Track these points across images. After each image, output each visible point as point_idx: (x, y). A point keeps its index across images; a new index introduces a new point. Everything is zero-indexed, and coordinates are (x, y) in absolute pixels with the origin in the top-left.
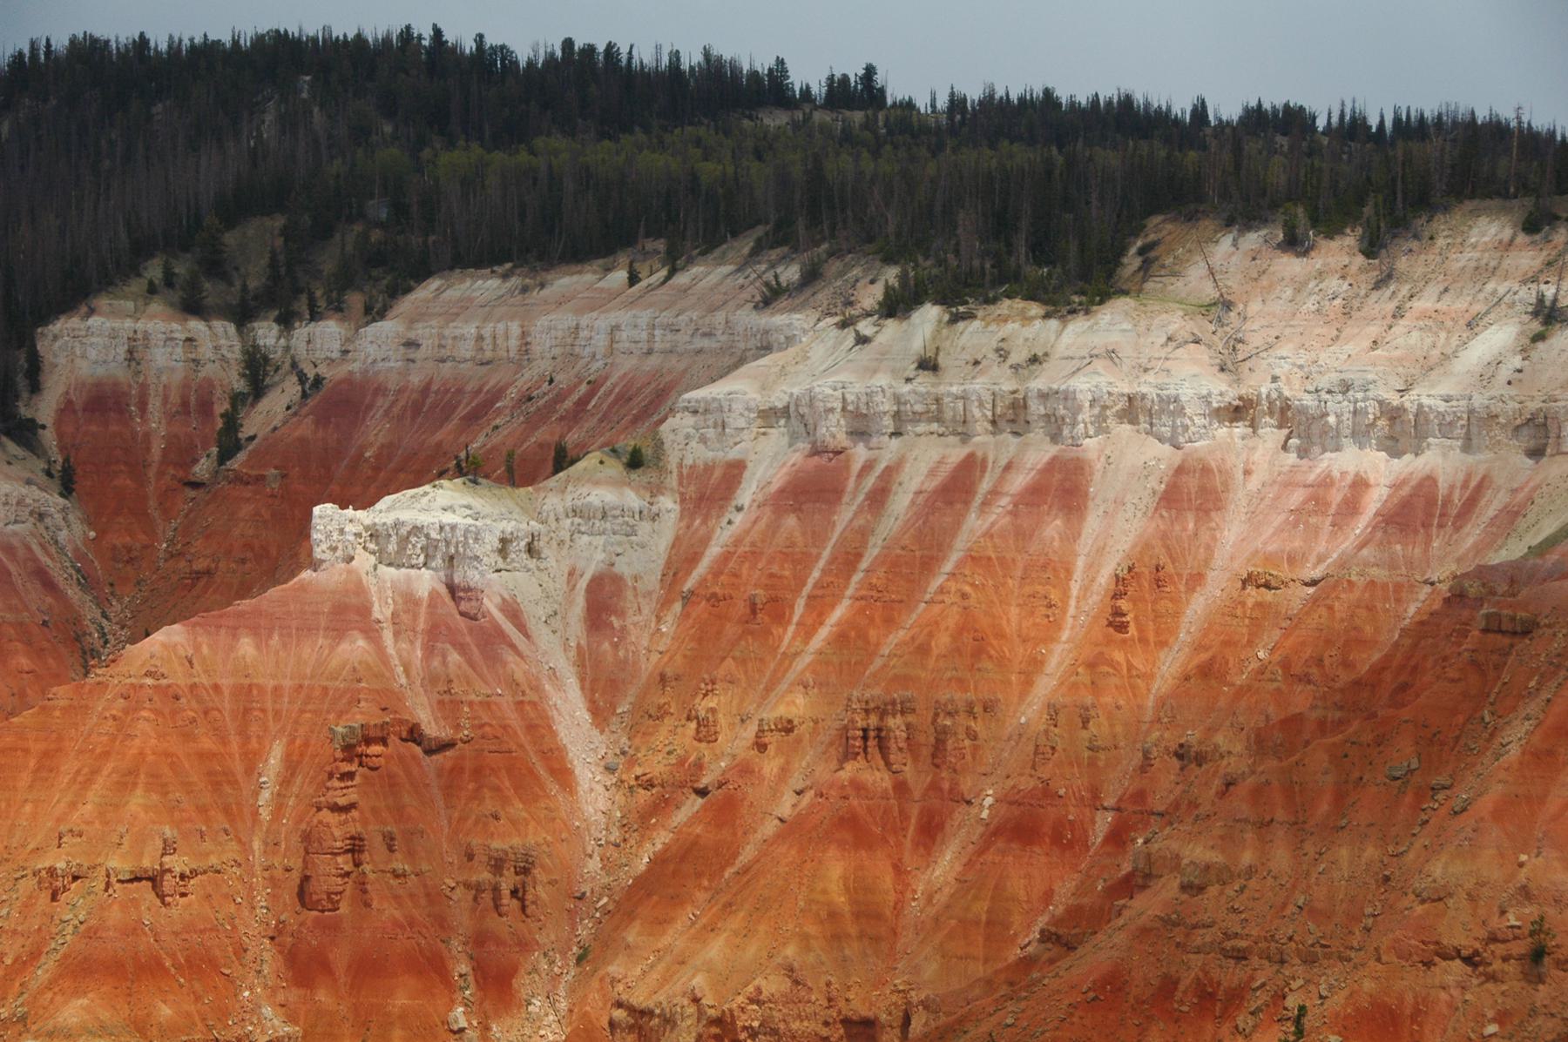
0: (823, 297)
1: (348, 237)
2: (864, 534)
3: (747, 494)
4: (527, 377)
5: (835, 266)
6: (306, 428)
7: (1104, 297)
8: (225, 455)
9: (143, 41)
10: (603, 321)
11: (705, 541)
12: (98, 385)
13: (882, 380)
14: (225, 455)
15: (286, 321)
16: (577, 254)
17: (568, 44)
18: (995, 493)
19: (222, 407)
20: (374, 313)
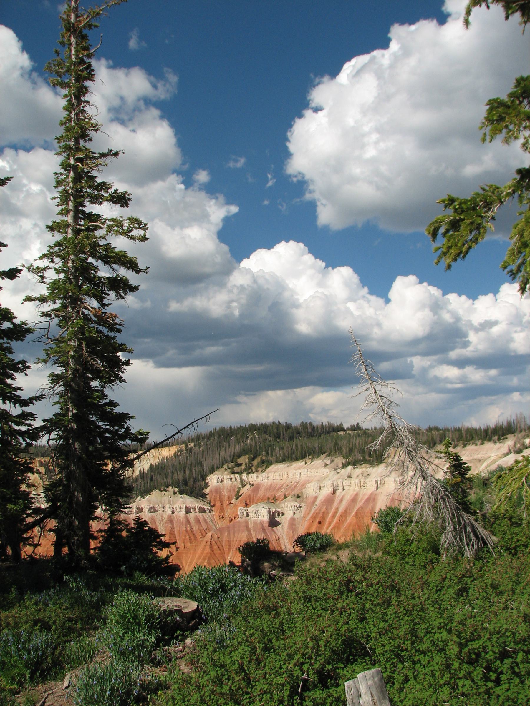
0: (333, 465)
1: (258, 459)
2: (337, 509)
3: (318, 502)
4: (287, 482)
5: (336, 459)
6: (250, 492)
7: (381, 462)
8: (237, 499)
9: (231, 427)
10: (298, 472)
11: (310, 511)
12: (216, 487)
13: (341, 480)
14: (237, 499)
15: (248, 474)
16: (297, 460)
17: (303, 422)
18: (362, 499)
19: (237, 490)
20: (262, 471)
